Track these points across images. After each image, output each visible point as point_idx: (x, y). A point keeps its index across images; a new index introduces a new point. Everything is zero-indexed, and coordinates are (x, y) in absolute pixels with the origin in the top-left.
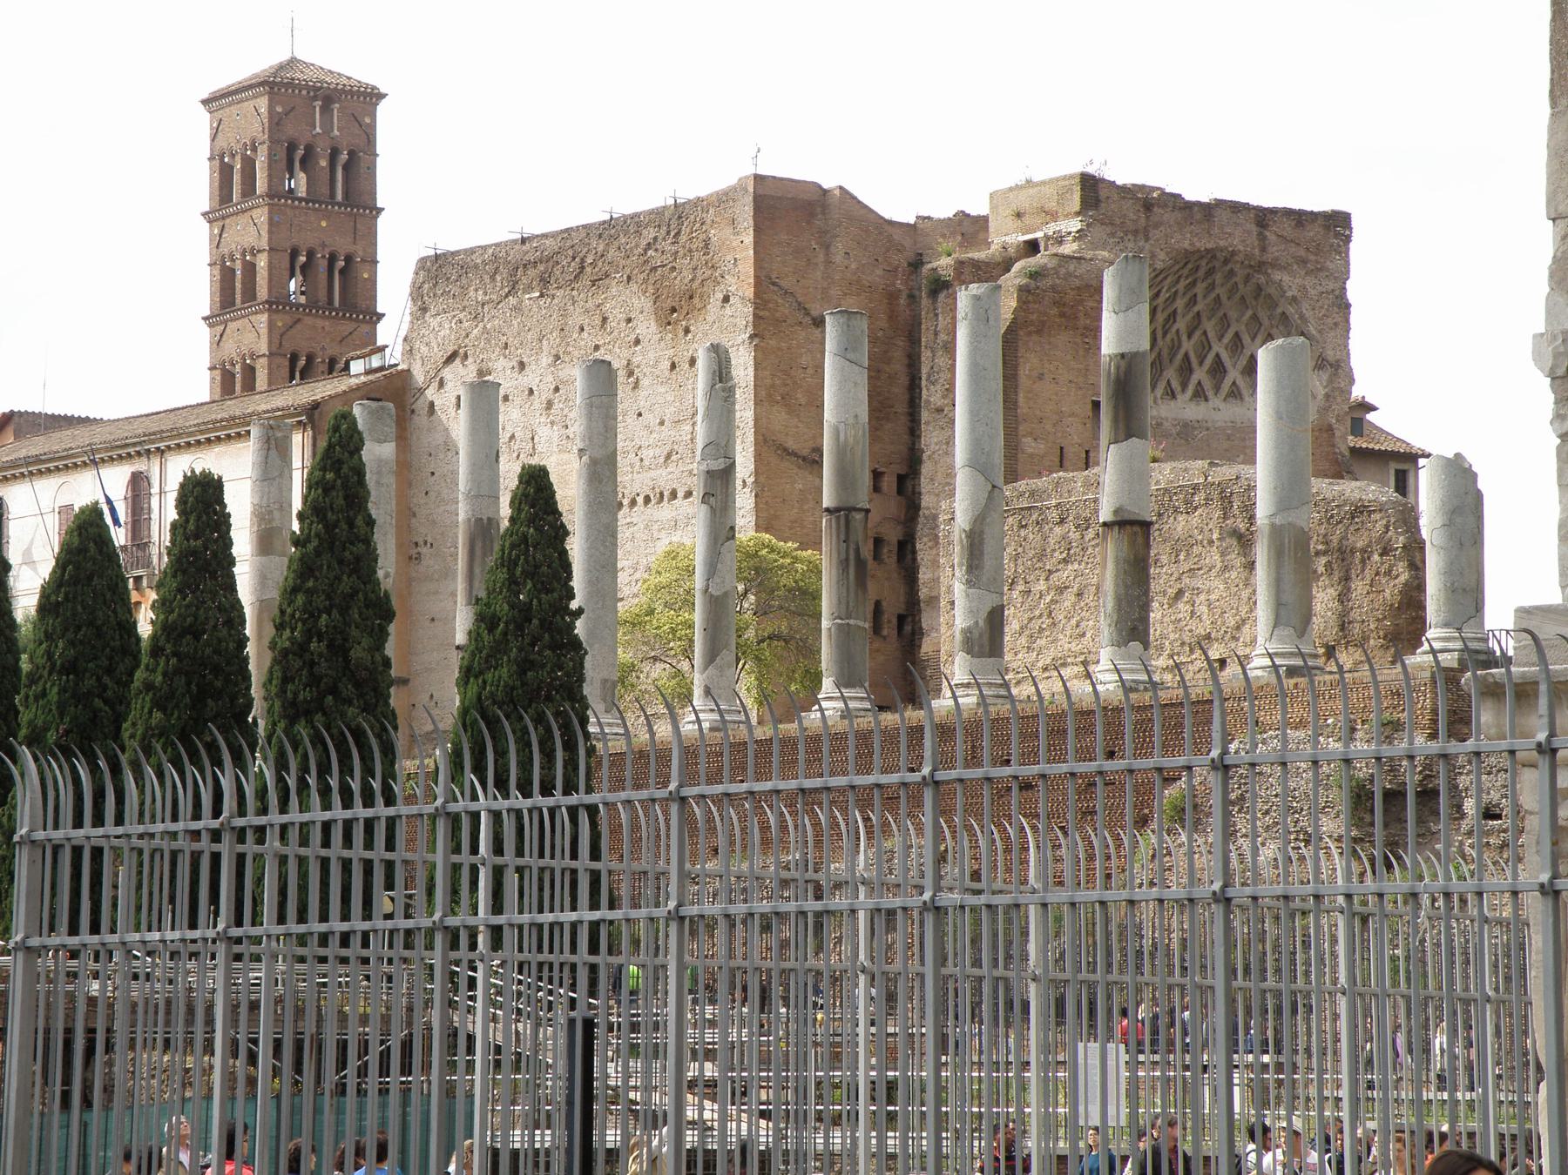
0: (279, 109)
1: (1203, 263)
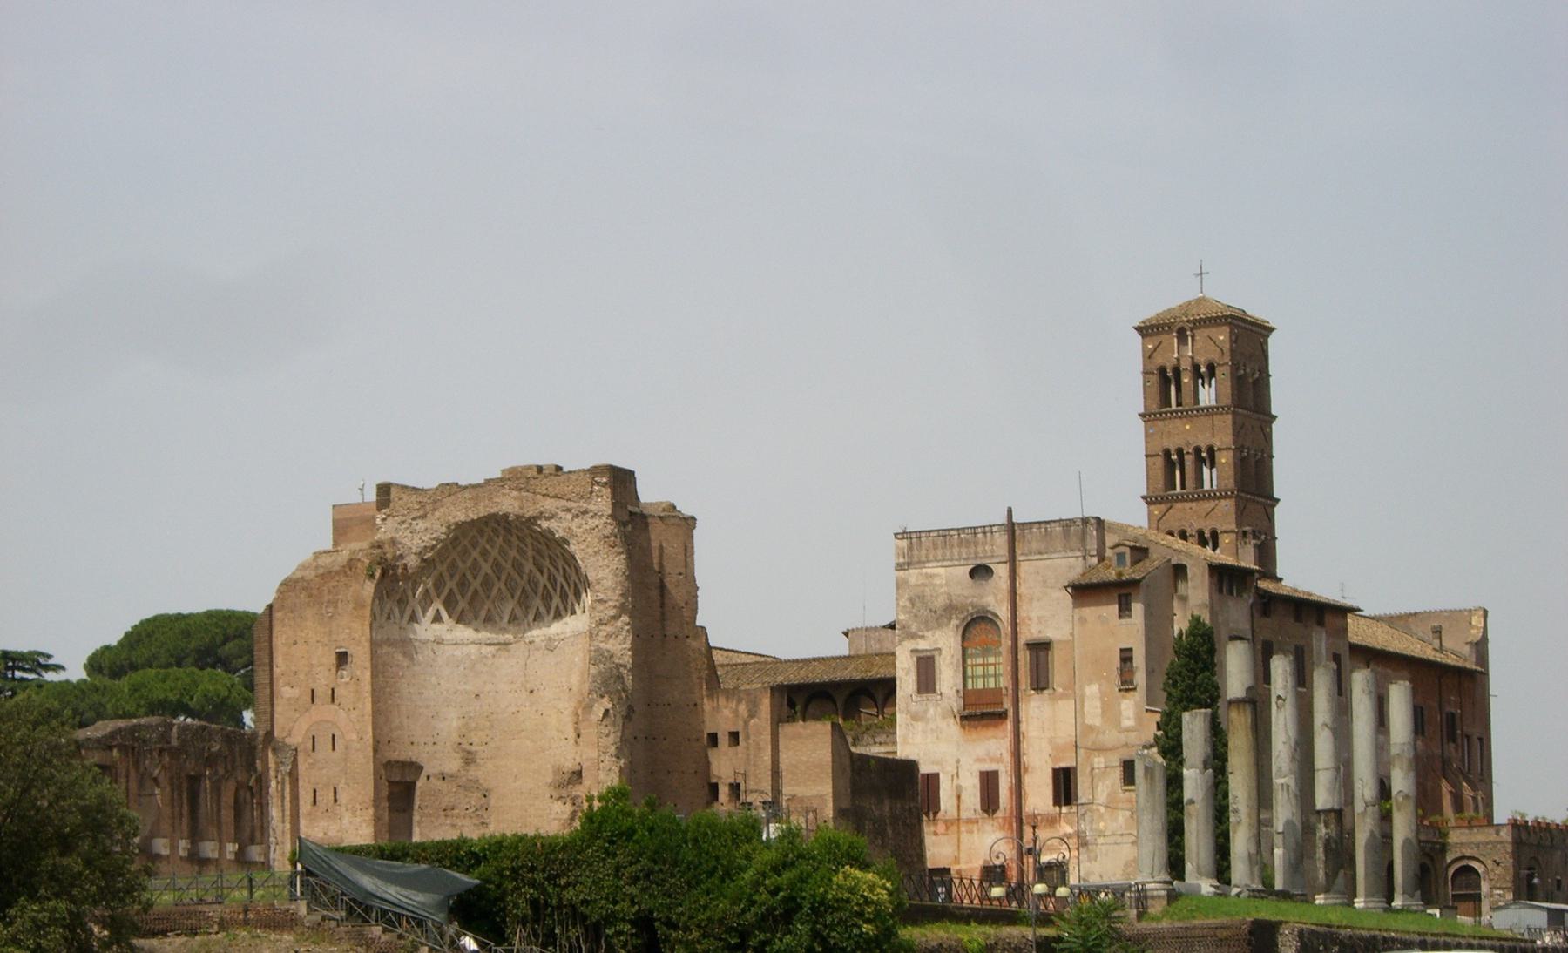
0: (1150, 346)
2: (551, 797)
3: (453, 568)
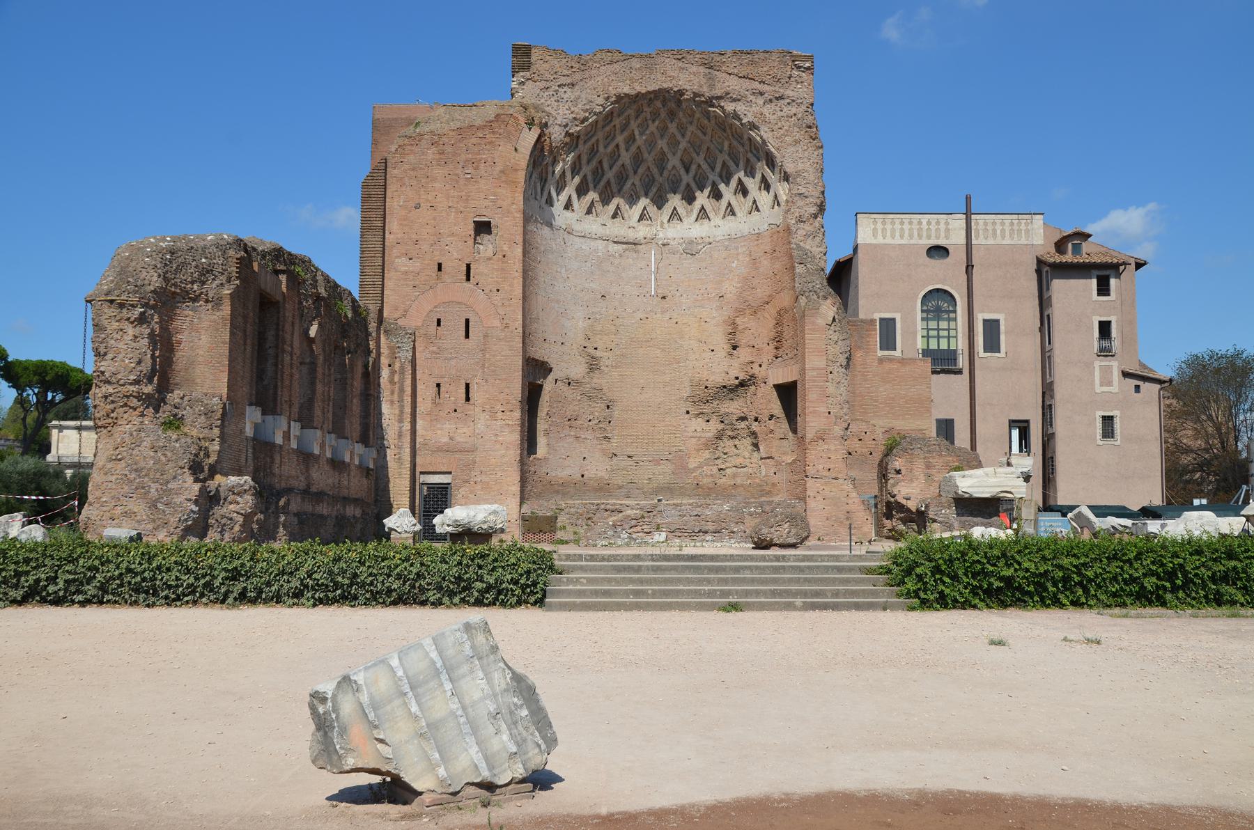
1: (658, 104)
2: (688, 412)
3: (593, 151)
